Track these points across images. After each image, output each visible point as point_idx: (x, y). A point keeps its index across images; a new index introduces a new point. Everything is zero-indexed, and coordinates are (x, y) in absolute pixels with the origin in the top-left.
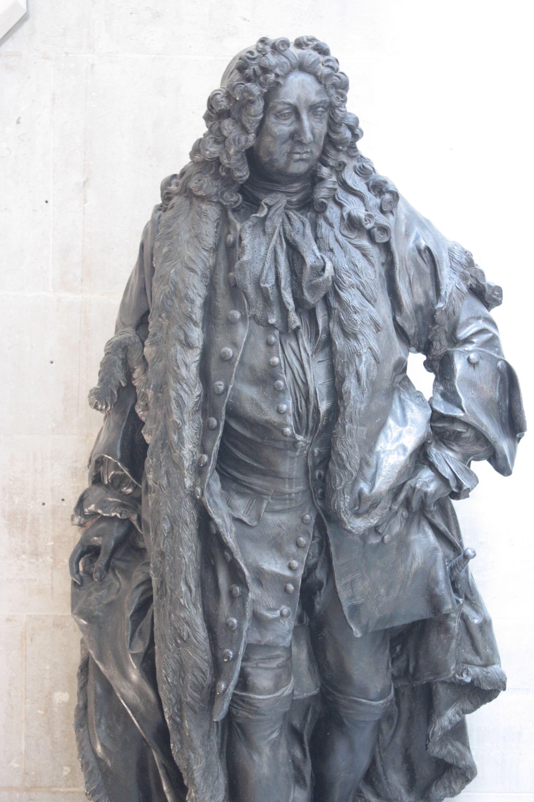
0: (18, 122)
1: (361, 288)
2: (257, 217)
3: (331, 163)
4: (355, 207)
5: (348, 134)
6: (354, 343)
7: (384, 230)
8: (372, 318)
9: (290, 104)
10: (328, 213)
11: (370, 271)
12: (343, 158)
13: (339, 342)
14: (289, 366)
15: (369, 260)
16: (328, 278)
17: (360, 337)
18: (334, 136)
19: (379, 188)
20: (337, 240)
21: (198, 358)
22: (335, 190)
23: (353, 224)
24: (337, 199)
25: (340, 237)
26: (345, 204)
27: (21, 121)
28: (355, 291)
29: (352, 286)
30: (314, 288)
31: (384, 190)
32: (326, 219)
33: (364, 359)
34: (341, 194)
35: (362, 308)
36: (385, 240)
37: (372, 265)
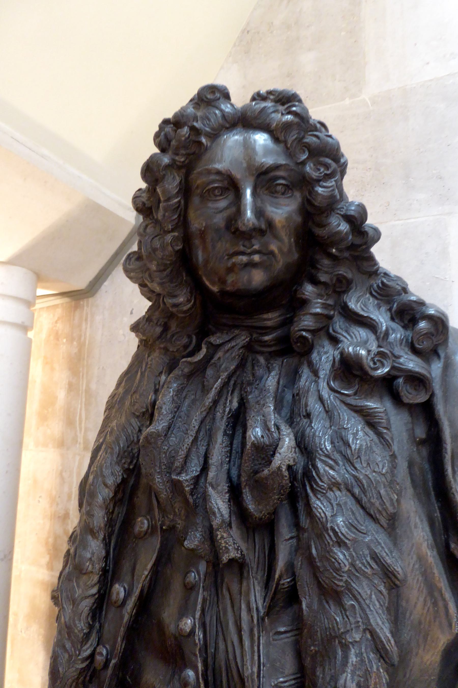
0: (131, 313)
1: (357, 491)
2: (190, 363)
3: (323, 278)
4: (358, 344)
5: (344, 227)
6: (333, 610)
7: (418, 381)
8: (375, 557)
9: (219, 173)
10: (314, 356)
11: (380, 456)
12: (344, 271)
13: (308, 602)
14: (223, 634)
15: (379, 435)
16: (279, 468)
17: (348, 602)
18: (319, 232)
19: (408, 313)
20: (321, 399)
21: (94, 590)
22: (330, 318)
23: (349, 370)
24: (331, 331)
25: (325, 393)
26: (342, 338)
27: (134, 312)
28: (340, 496)
29: (335, 485)
30: (260, 486)
31: (418, 316)
32: (310, 364)
33: (353, 659)
34: (339, 325)
35: (351, 535)
36: (422, 398)
37: (386, 443)
